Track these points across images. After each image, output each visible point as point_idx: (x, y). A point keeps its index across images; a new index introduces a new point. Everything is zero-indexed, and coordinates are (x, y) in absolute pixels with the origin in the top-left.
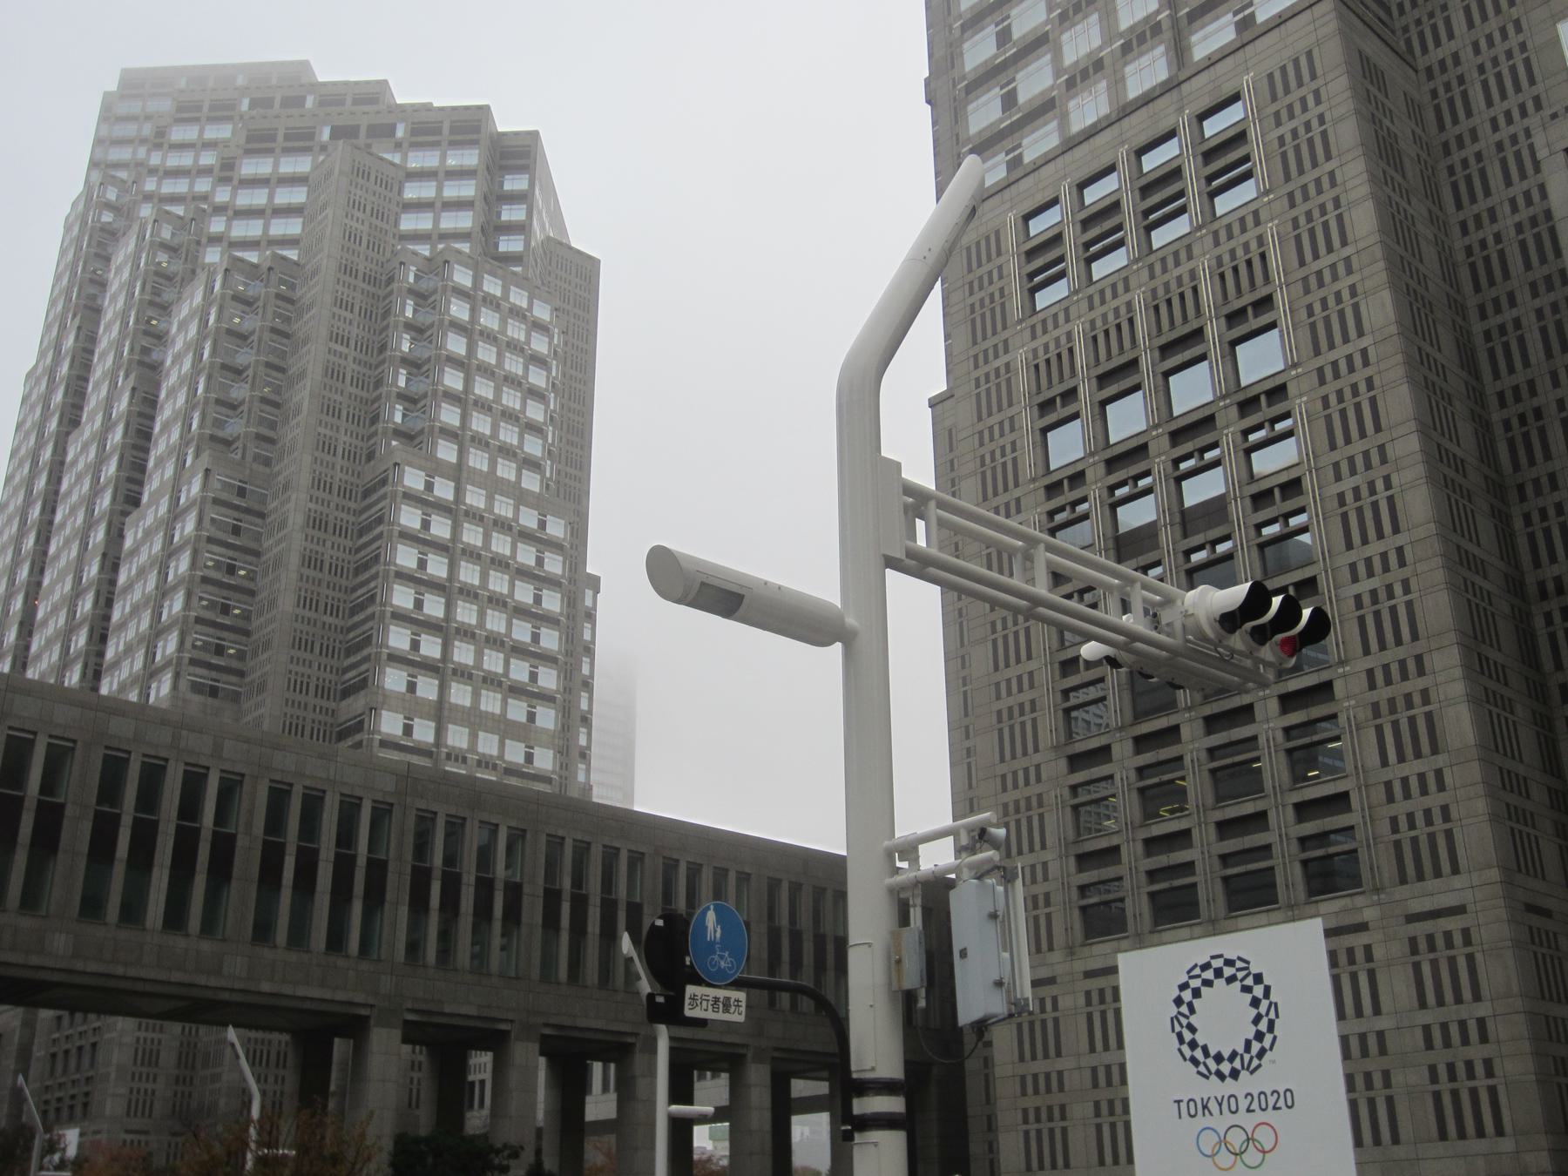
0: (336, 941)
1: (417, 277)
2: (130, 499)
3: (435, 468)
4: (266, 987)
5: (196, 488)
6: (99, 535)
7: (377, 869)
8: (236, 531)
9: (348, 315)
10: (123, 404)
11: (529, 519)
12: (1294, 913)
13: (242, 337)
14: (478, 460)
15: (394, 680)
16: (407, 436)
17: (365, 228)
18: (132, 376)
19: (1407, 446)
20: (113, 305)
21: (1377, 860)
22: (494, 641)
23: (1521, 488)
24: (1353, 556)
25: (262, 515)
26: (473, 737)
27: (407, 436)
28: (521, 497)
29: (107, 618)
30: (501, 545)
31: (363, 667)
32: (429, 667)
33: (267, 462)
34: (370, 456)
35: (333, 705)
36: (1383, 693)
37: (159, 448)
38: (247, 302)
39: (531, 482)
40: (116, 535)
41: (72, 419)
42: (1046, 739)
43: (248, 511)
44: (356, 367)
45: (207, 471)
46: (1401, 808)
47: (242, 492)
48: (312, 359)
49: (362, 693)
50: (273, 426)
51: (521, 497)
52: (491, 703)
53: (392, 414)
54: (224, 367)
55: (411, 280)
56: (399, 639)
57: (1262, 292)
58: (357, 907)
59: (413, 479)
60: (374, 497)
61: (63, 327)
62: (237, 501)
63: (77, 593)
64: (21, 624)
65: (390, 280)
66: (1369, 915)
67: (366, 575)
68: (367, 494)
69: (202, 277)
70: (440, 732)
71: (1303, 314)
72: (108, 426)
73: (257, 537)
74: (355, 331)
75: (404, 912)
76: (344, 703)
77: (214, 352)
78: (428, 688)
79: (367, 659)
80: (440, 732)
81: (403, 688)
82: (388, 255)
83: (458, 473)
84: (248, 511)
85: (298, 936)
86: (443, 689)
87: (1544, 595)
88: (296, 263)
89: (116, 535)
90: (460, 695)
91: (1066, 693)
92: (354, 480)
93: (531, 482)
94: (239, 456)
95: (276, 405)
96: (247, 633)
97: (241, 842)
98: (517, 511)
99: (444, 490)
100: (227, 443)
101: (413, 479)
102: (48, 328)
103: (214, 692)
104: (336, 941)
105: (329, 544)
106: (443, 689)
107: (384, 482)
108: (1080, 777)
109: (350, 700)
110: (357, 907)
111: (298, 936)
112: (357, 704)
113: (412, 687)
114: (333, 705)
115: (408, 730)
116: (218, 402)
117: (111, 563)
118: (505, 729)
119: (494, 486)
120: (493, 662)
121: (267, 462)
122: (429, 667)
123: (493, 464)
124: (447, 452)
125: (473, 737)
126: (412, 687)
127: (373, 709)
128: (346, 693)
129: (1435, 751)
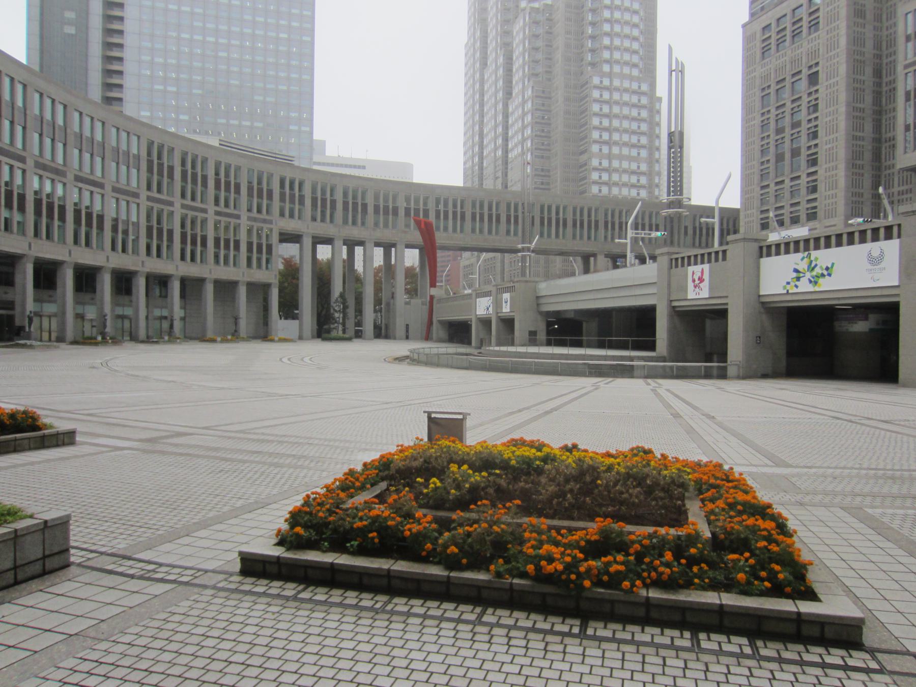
0: (589, 238)
1: (592, 4)
2: (508, 94)
3: (603, 75)
4: (576, 249)
5: (530, 92)
6: (500, 106)
7: (597, 222)
8: (543, 105)
10: (501, 60)
11: (635, 86)
12: (803, 226)
13: (536, 36)
14: (616, 69)
15: (595, 148)
16: (593, 65)
18: (503, 49)
19: (843, 109)
20: (492, 23)
21: (820, 214)
22: (626, 131)
23: (886, 111)
24: (826, 139)
25: (550, 98)
26: (621, 163)
27: (593, 65)
28: (631, 78)
29: (483, 100)
30: (626, 97)
32: (606, 143)
33: (549, 80)
34: (582, 73)
36: (828, 174)
37: (515, 79)
38: (536, 23)
39: (635, 72)
40: (506, 106)
41: (484, 64)
42: (756, 182)
43: (546, 98)
45: (533, 87)
46: (827, 201)
48: (559, 42)
50: (550, 67)
51: (631, 78)
52: (625, 151)
54: (533, 48)
55: (590, 5)
56: (595, 135)
57: (816, 61)
58: (593, 230)
59: (596, 80)
60: (584, 88)
61: (475, 28)
62: (542, 95)
63: (496, 126)
64: (479, 134)
65: (583, 7)
66: (817, 226)
67: (584, 115)
68: (582, 86)
69: (521, 16)
70: (610, 163)
71: (825, 68)
72: (497, 69)
75: (603, 231)
77: (529, 43)
78: (605, 149)
79: (586, 142)
80: (610, 163)
81: (598, 151)
83: (610, 75)
84: (546, 98)
85: (581, 237)
86: (610, 149)
87: (886, 141)
88: (551, 5)
89: (506, 106)
90: (616, 150)
91: (762, 170)
93: (635, 72)
94: (541, 79)
95: (550, 59)
96: (550, 137)
98: (631, 84)
99: (606, 82)
100: (537, 75)
101: (596, 80)
102: (469, 29)
103: (542, 157)
104: (589, 238)
106: (610, 149)
107: (587, 83)
108: (763, 192)
109: (582, 156)
110: (593, 230)
111: (581, 237)
112: (584, 157)
113: (601, 150)
115: (600, 164)
116: (533, 61)
117: (506, 116)
118: (630, 159)
119: (622, 76)
120: (626, 138)
121: (549, 80)
122: (606, 143)
123: (622, 69)
124: (606, 68)
125: (621, 163)
126: (601, 150)
127: (590, 159)
128: (582, 153)
129: (836, 188)
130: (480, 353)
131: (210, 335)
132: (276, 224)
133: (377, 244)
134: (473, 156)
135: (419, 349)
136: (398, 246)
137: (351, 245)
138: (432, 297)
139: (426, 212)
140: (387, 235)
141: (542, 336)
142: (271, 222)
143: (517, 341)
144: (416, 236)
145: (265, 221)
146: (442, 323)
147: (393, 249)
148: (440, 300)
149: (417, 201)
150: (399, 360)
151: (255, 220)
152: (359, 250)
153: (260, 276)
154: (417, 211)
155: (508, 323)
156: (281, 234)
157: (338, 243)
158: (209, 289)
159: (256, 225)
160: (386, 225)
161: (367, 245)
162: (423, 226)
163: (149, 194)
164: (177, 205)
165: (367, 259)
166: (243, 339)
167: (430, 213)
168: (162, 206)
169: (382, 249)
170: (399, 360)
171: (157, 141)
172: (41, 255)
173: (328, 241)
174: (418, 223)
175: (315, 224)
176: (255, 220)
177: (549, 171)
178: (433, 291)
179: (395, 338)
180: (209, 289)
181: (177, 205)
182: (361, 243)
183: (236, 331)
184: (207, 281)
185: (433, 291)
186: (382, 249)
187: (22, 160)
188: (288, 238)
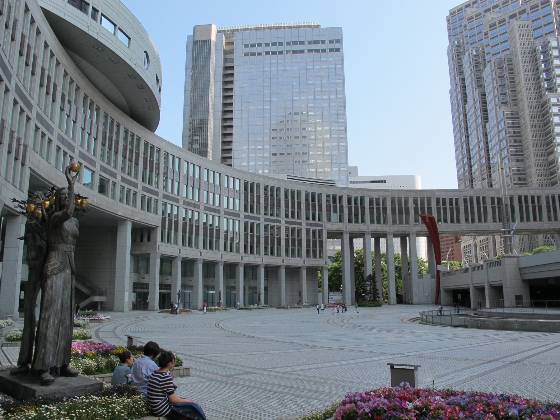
1: (542, 48)
2: (486, 119)
8: (513, 123)
9: (527, 64)
17: (525, 40)
31: (552, 148)
33: (516, 105)
35: (546, 158)
43: (515, 118)
44: (532, 76)
47: (512, 114)
49: (553, 154)
53: (543, 76)
55: (541, 49)
73: (518, 123)
74: (529, 67)
76: (549, 157)
82: (533, 44)
84: (515, 118)
92: (539, 104)
97: (543, 206)
103: (517, 161)
105: (536, 121)
109: (550, 156)
114: (546, 158)
121: (516, 105)
130: (476, 314)
131: (283, 303)
132: (325, 227)
133: (396, 235)
134: (464, 165)
135: (428, 312)
136: (411, 236)
137: (377, 237)
138: (438, 272)
139: (430, 209)
140: (403, 228)
141: (526, 300)
142: (321, 225)
143: (506, 304)
144: (424, 228)
145: (317, 225)
146: (447, 291)
147: (408, 238)
148: (446, 274)
149: (422, 201)
150: (414, 320)
151: (311, 225)
152: (383, 241)
153: (314, 262)
154: (423, 209)
155: (498, 290)
156: (328, 233)
157: (368, 237)
158: (283, 272)
159: (311, 228)
160: (401, 222)
161: (389, 236)
162: (427, 220)
163: (246, 213)
164: (262, 219)
165: (389, 246)
166: (305, 306)
167: (433, 210)
168: (253, 221)
169: (399, 239)
170: (414, 320)
171: (250, 181)
172: (185, 256)
173: (361, 235)
174: (424, 218)
175: (351, 224)
176: (311, 225)
177: (524, 170)
178: (439, 267)
179: (412, 304)
180: (283, 272)
181: (262, 219)
182: (385, 235)
183: (300, 301)
184: (281, 267)
185: (439, 267)
186: (399, 239)
187: (177, 201)
188: (332, 235)
